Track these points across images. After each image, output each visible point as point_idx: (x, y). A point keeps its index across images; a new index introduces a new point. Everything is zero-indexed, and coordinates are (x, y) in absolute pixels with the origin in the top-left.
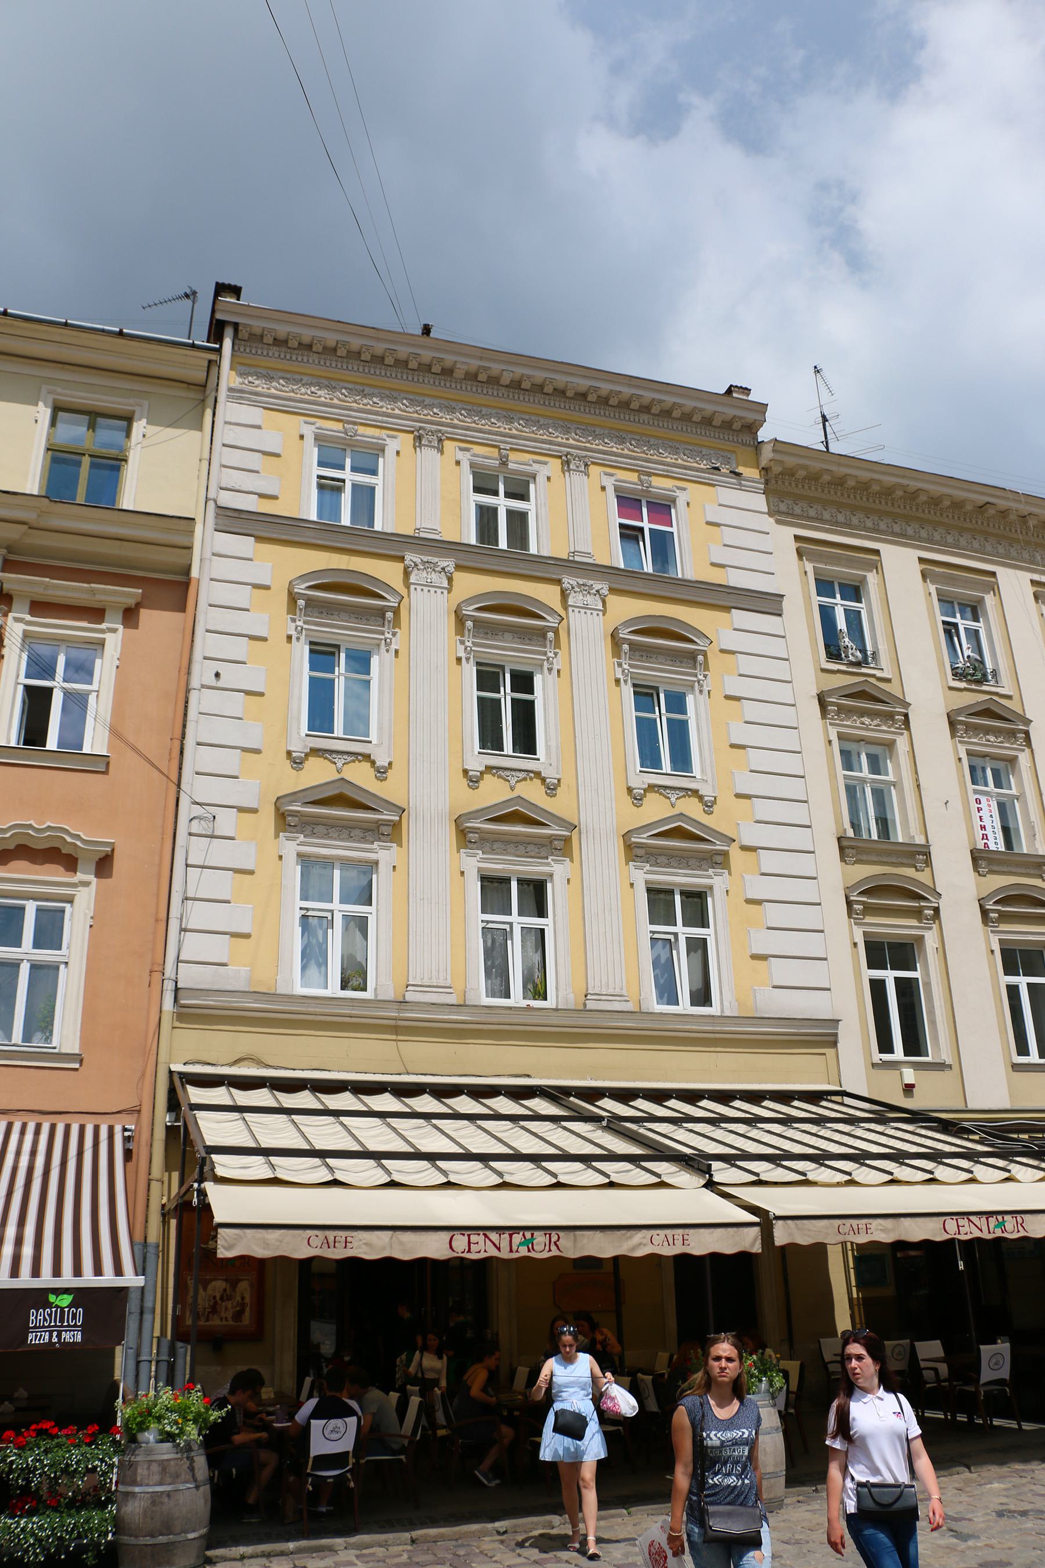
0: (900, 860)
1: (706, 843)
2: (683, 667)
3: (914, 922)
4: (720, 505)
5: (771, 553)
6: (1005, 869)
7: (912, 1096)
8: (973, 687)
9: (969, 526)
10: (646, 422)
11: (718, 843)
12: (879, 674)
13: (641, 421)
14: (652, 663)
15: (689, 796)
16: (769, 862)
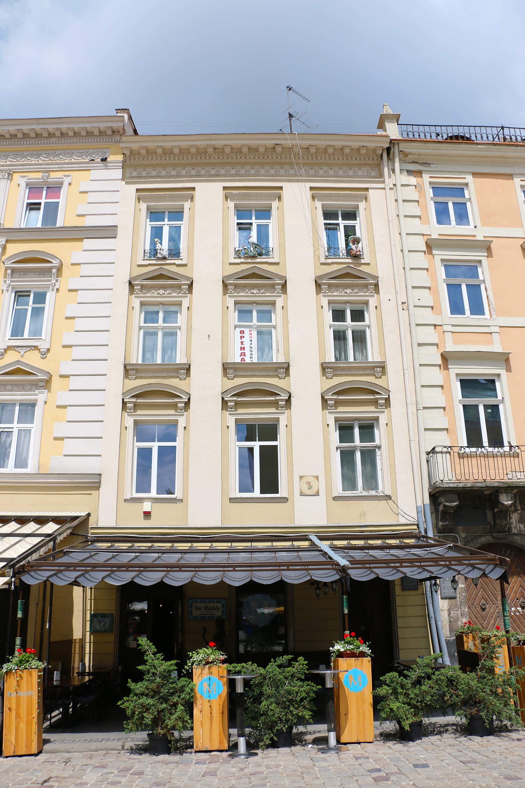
0: (169, 374)
1: (32, 375)
2: (45, 277)
3: (173, 412)
4: (91, 180)
5: (118, 202)
6: (249, 374)
7: (150, 519)
8: (249, 261)
9: (268, 161)
10: (54, 142)
11: (39, 375)
12: (177, 262)
13: (51, 143)
14: (26, 278)
15: (33, 350)
16: (74, 384)
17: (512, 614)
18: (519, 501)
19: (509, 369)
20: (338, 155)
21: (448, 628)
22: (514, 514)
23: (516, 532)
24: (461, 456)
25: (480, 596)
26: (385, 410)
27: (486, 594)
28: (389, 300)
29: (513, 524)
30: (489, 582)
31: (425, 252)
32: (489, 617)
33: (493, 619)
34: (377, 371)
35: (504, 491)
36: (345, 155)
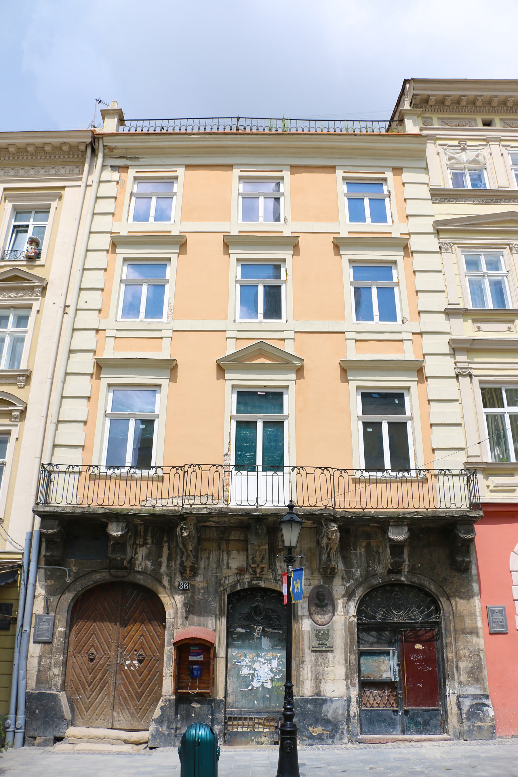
17: (126, 668)
18: (151, 533)
19: (173, 378)
20: (41, 153)
21: (35, 678)
22: (141, 548)
23: (140, 570)
24: (94, 478)
25: (90, 643)
26: (19, 423)
27: (98, 642)
28: (54, 303)
29: (138, 560)
30: (104, 628)
31: (108, 251)
32: (97, 669)
33: (101, 672)
34: (19, 380)
35: (114, 520)
36: (48, 154)
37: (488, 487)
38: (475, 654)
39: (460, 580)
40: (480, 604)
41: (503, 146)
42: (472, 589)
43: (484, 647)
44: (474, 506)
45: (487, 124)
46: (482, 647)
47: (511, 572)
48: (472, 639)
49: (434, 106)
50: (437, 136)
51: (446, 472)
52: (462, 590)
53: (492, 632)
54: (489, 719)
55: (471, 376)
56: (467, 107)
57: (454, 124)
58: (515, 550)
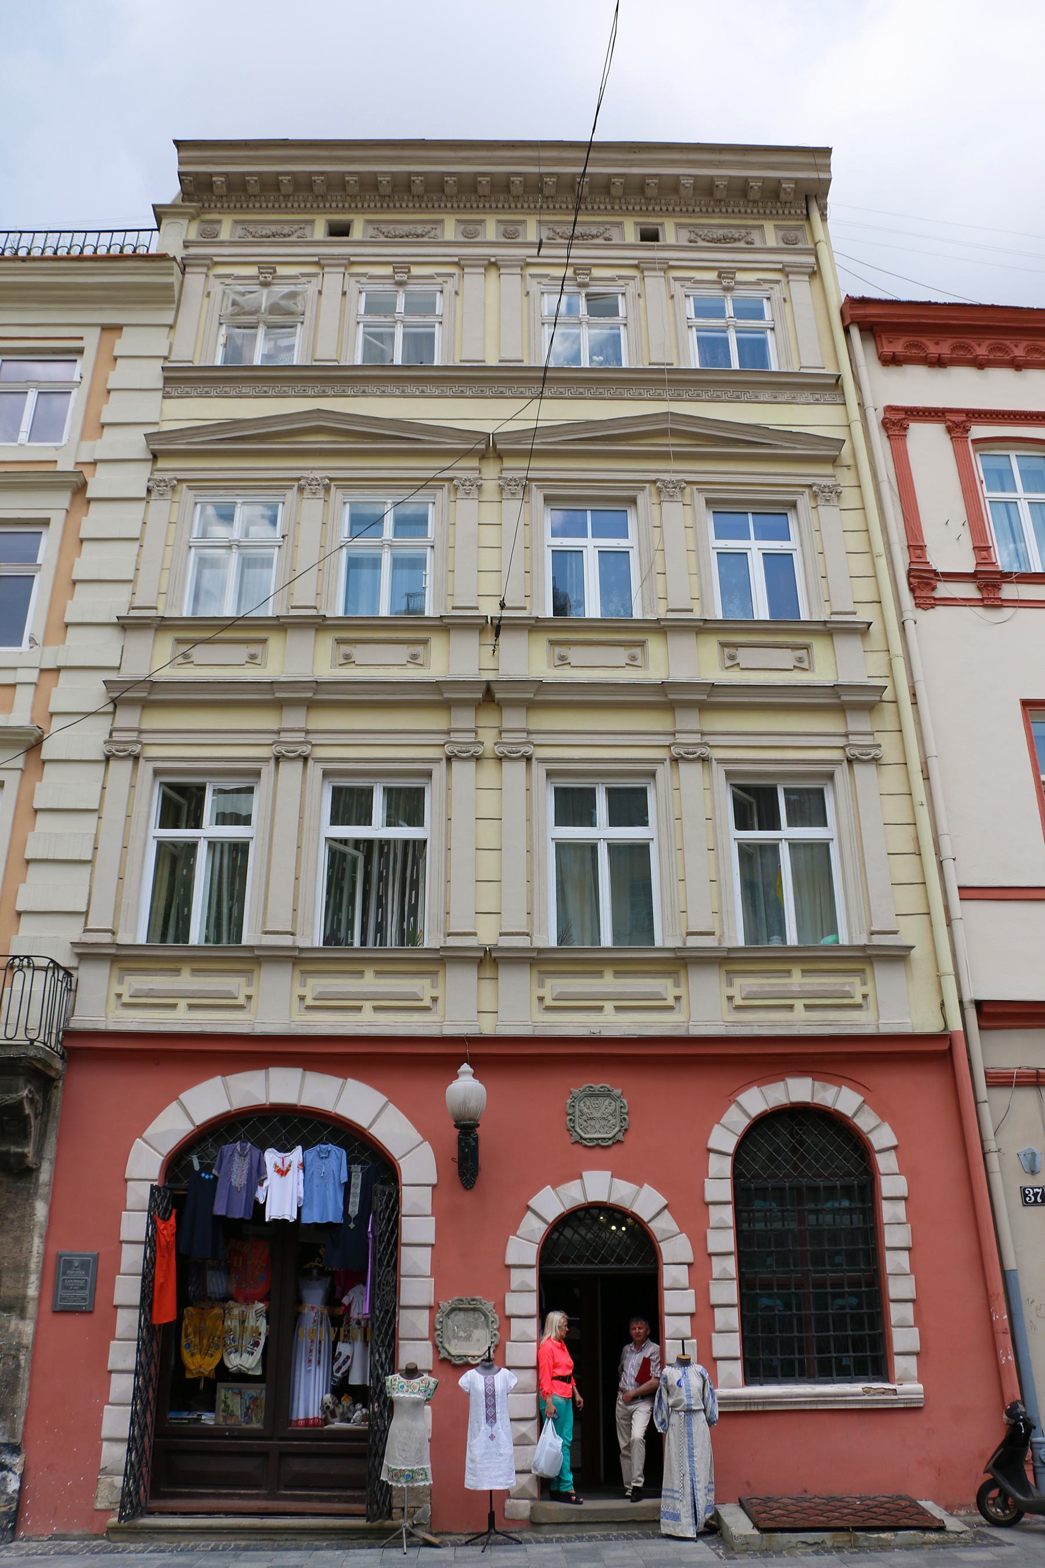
37: (119, 996)
38: (9, 1355)
39: (11, 1192)
40: (41, 1247)
41: (352, 275)
42: (32, 1214)
43: (30, 1341)
44: (69, 1034)
45: (339, 230)
46: (27, 1339)
47: (126, 1181)
48: (9, 1321)
49: (226, 196)
50: (216, 259)
51: (27, 963)
52: (11, 1216)
53: (58, 1309)
54: (5, 1497)
55: (136, 758)
56: (296, 198)
57: (264, 233)
58: (144, 1135)
